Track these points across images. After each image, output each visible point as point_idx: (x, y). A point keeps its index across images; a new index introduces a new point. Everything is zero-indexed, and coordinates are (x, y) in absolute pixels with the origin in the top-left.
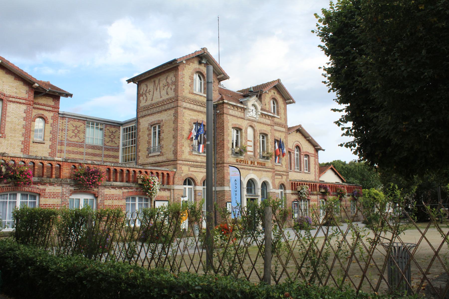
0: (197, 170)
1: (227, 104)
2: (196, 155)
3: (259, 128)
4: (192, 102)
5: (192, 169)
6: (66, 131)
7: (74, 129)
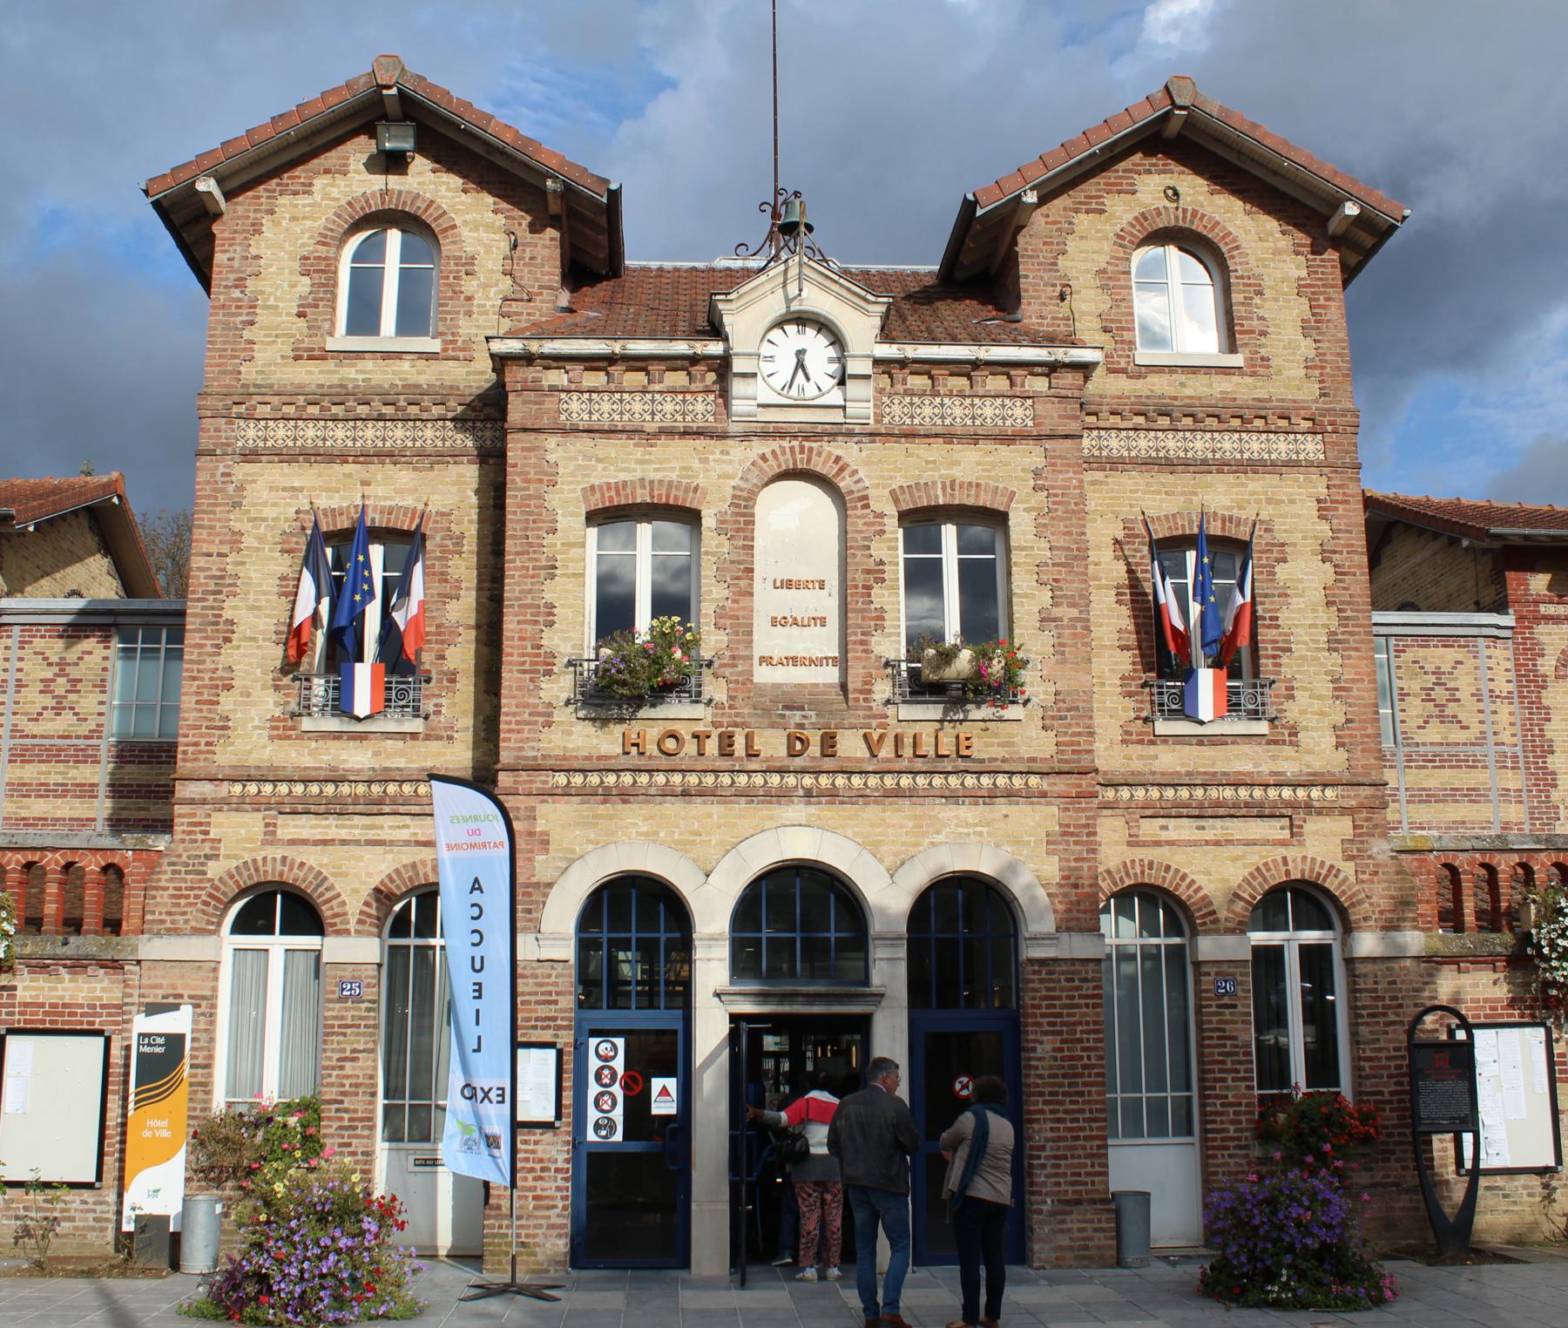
0: (343, 834)
1: (528, 359)
2: (336, 736)
3: (885, 475)
4: (314, 410)
5: (291, 828)
6: (11, 688)
7: (49, 674)
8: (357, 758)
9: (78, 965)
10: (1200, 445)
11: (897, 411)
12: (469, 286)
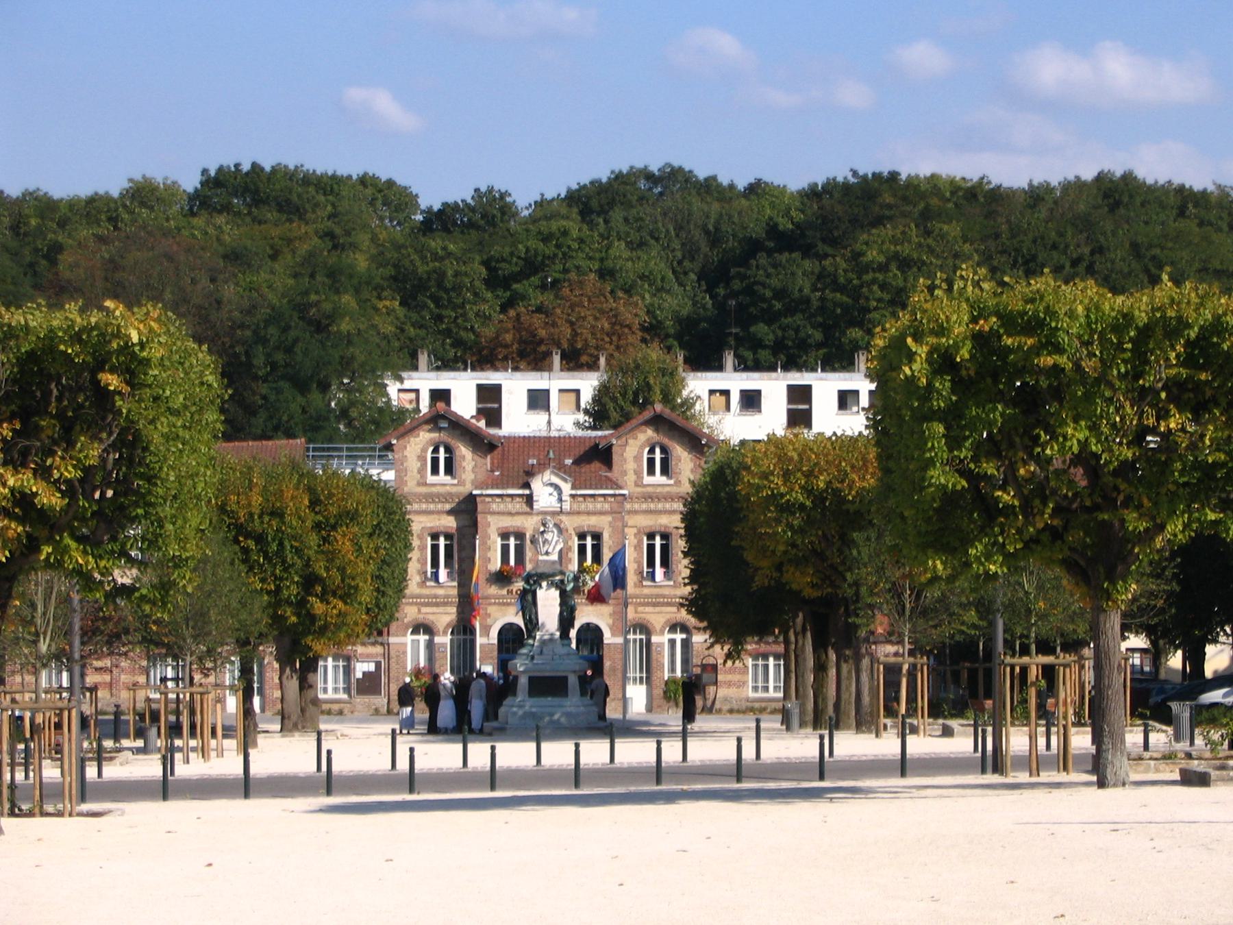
1: (481, 495)
3: (570, 523)
5: (424, 610)
8: (441, 592)
9: (373, 644)
10: (660, 506)
11: (575, 506)
12: (464, 464)
